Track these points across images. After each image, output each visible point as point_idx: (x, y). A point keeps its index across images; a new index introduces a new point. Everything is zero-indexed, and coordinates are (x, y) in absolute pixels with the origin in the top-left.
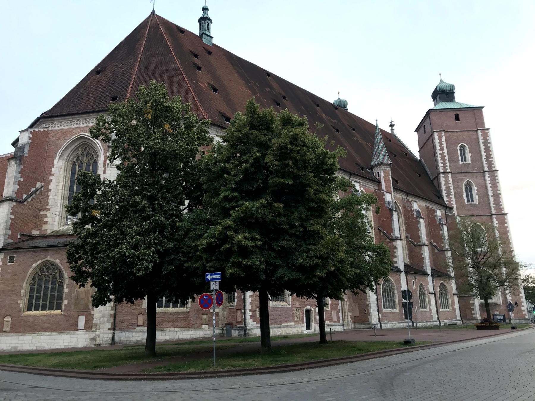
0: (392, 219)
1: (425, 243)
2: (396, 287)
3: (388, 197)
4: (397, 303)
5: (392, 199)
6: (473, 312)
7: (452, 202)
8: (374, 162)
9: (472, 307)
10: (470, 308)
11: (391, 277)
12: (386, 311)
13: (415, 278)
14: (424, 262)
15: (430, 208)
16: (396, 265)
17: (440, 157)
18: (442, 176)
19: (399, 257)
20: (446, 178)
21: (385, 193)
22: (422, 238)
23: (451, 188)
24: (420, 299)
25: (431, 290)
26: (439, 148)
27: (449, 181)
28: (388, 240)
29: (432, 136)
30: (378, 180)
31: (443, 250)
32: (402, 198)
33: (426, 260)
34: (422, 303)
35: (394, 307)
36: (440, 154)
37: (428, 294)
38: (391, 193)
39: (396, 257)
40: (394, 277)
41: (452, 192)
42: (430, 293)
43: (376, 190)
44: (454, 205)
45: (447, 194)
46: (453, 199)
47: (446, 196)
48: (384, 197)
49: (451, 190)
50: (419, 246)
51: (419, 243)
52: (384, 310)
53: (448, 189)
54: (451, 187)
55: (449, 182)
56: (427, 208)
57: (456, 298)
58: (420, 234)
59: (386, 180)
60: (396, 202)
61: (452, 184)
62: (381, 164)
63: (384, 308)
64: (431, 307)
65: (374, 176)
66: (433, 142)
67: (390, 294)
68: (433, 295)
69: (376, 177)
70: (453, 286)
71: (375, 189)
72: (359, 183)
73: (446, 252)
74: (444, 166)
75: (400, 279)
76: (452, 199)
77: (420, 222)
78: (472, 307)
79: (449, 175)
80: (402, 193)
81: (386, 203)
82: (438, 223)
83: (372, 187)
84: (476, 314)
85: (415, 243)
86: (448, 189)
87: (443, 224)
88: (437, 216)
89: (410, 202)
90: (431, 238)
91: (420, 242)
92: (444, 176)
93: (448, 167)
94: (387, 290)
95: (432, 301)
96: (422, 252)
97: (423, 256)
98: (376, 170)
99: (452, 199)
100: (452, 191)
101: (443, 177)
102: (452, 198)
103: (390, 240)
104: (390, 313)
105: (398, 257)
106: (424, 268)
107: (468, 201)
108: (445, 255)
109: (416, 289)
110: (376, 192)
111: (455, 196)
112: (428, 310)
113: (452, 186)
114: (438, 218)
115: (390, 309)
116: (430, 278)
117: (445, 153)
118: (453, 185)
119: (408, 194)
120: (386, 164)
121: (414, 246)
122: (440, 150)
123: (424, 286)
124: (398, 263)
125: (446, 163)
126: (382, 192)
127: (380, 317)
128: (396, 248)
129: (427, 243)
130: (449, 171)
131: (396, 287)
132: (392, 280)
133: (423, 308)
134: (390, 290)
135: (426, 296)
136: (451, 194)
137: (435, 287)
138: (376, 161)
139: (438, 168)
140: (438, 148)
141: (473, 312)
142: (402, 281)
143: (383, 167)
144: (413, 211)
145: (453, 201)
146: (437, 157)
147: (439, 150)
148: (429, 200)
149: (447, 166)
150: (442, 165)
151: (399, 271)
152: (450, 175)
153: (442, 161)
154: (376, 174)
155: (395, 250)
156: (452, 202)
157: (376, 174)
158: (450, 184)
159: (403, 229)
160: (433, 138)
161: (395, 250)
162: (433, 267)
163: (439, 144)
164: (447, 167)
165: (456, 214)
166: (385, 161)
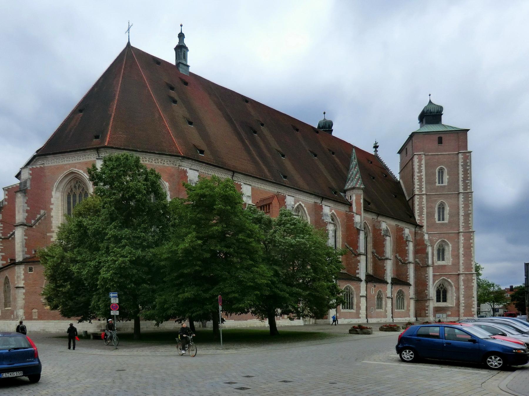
0: (359, 238)
1: (388, 257)
2: (355, 293)
3: (357, 219)
4: (355, 305)
5: (361, 220)
7: (423, 221)
8: (348, 186)
11: (351, 285)
12: (344, 311)
13: (375, 286)
14: (385, 273)
15: (399, 227)
16: (357, 276)
17: (417, 180)
18: (416, 197)
19: (362, 269)
20: (421, 199)
21: (355, 214)
22: (386, 253)
23: (424, 208)
24: (377, 302)
25: (389, 295)
26: (418, 171)
27: (423, 202)
28: (353, 255)
29: (412, 159)
30: (349, 203)
31: (406, 262)
32: (373, 218)
33: (388, 271)
34: (379, 306)
35: (352, 309)
36: (418, 176)
37: (385, 298)
38: (360, 215)
39: (358, 269)
40: (354, 285)
41: (424, 212)
42: (387, 298)
43: (347, 212)
44: (425, 224)
46: (425, 218)
48: (353, 218)
49: (424, 210)
50: (382, 259)
51: (383, 258)
52: (342, 310)
53: (421, 209)
54: (424, 207)
55: (423, 203)
56: (397, 227)
57: (412, 303)
58: (385, 250)
59: (358, 203)
60: (366, 222)
61: (425, 204)
62: (353, 188)
63: (342, 308)
64: (386, 308)
65: (347, 199)
66: (413, 165)
67: (350, 298)
68: (391, 299)
69: (348, 200)
70: (411, 291)
71: (346, 211)
72: (329, 206)
73: (408, 264)
74: (420, 189)
75: (360, 286)
76: (423, 218)
77: (386, 239)
79: (423, 196)
80: (373, 214)
81: (355, 223)
82: (405, 240)
83: (343, 209)
85: (380, 257)
86: (421, 209)
87: (409, 241)
88: (404, 234)
89: (380, 222)
90: (397, 252)
91: (384, 256)
92: (418, 197)
93: (424, 189)
94: (347, 295)
95: (388, 304)
96: (385, 265)
97: (385, 268)
98: (348, 194)
99: (423, 218)
100: (425, 211)
101: (418, 198)
102: (423, 217)
103: (355, 255)
104: (347, 312)
105: (360, 269)
106: (385, 278)
107: (439, 220)
108: (408, 267)
109: (374, 294)
110: (347, 213)
111: (427, 216)
112: (384, 311)
113: (425, 206)
114: (406, 235)
115: (347, 310)
116: (389, 286)
117: (422, 175)
118: (427, 205)
119: (378, 215)
120: (359, 188)
121: (378, 260)
122: (418, 173)
123: (382, 292)
124: (359, 274)
125: (423, 185)
126: (352, 213)
127: (338, 315)
128: (359, 262)
129: (390, 258)
130: (424, 192)
131: (355, 293)
132: (353, 288)
133: (379, 309)
134: (349, 295)
135: (384, 300)
136: (424, 213)
137: (393, 293)
138: (349, 185)
139: (414, 189)
140: (416, 170)
142: (361, 289)
143: (355, 191)
144: (381, 230)
145: (424, 220)
146: (415, 179)
147: (417, 172)
148: (399, 220)
149: (423, 188)
150: (418, 187)
151: (360, 280)
152: (424, 197)
153: (418, 183)
154: (348, 197)
155: (358, 264)
156: (423, 221)
157: (348, 197)
158: (424, 204)
159: (370, 245)
160: (413, 161)
161: (358, 264)
162: (396, 277)
163: (418, 167)
164: (423, 189)
165: (425, 232)
166: (357, 186)
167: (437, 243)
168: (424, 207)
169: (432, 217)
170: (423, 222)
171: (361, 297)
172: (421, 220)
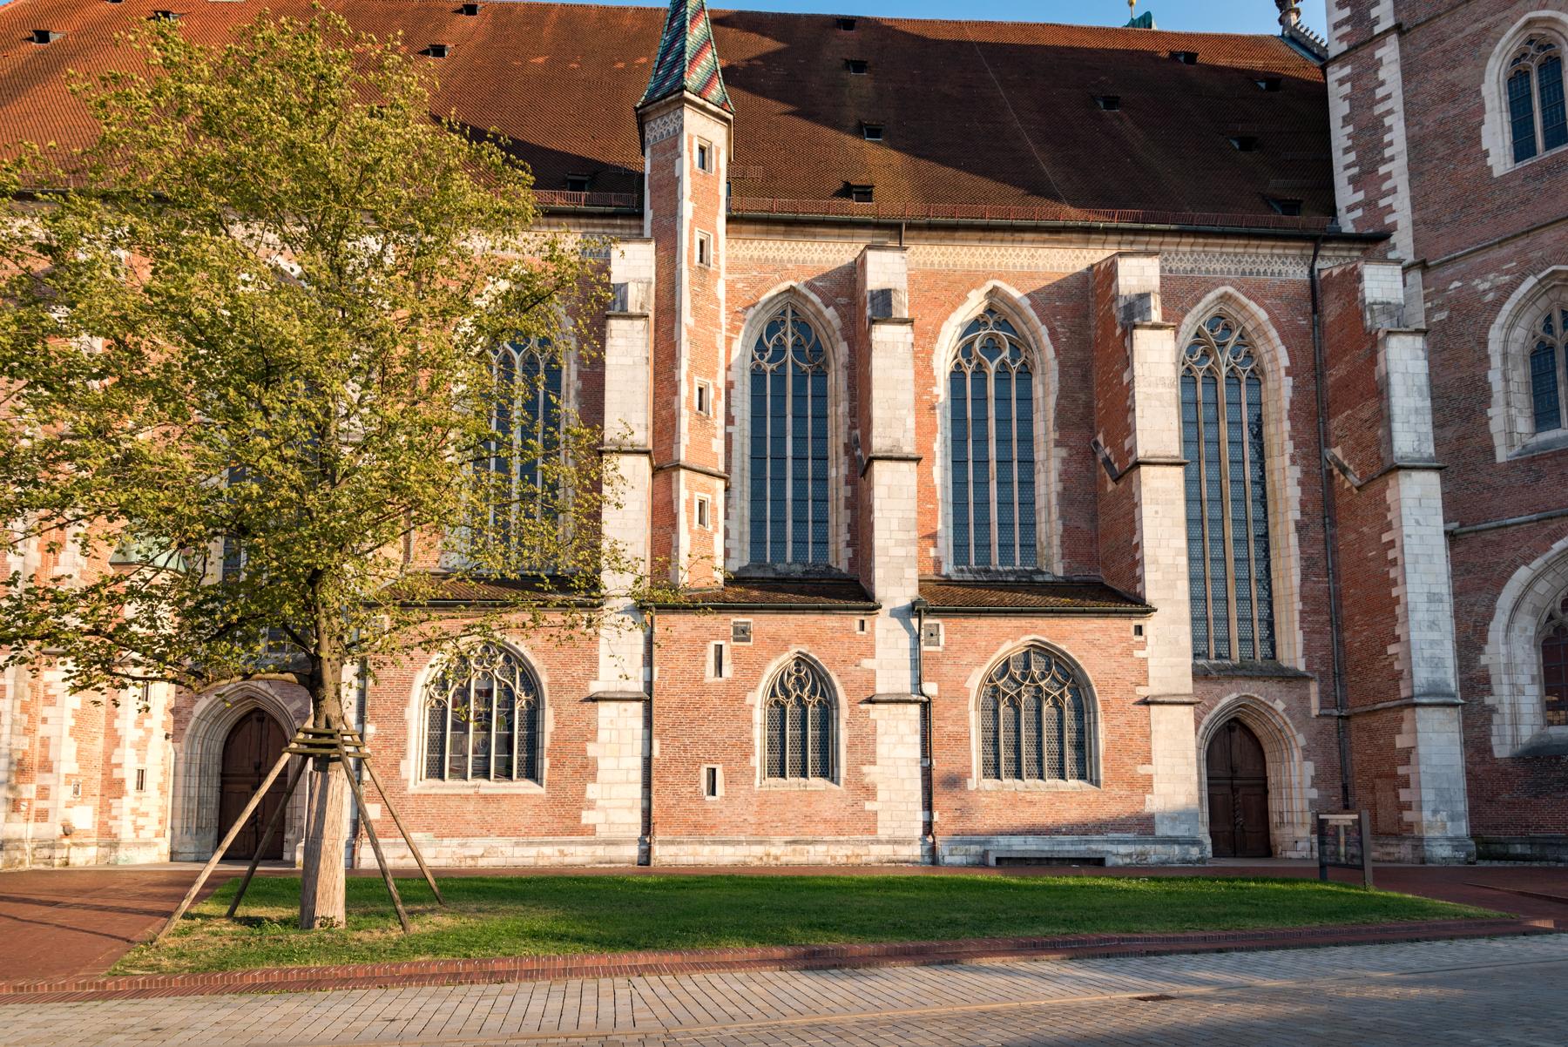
6: (1404, 795)
9: (1401, 770)
10: (1394, 776)
45: (1355, 170)
47: (1353, 180)
78: (1401, 770)
84: (1420, 809)
141: (1404, 795)
167: (1508, 307)
168: (1390, 112)
169: (1461, 155)
170: (1389, 209)
171: (594, 699)
172: (1369, 204)
